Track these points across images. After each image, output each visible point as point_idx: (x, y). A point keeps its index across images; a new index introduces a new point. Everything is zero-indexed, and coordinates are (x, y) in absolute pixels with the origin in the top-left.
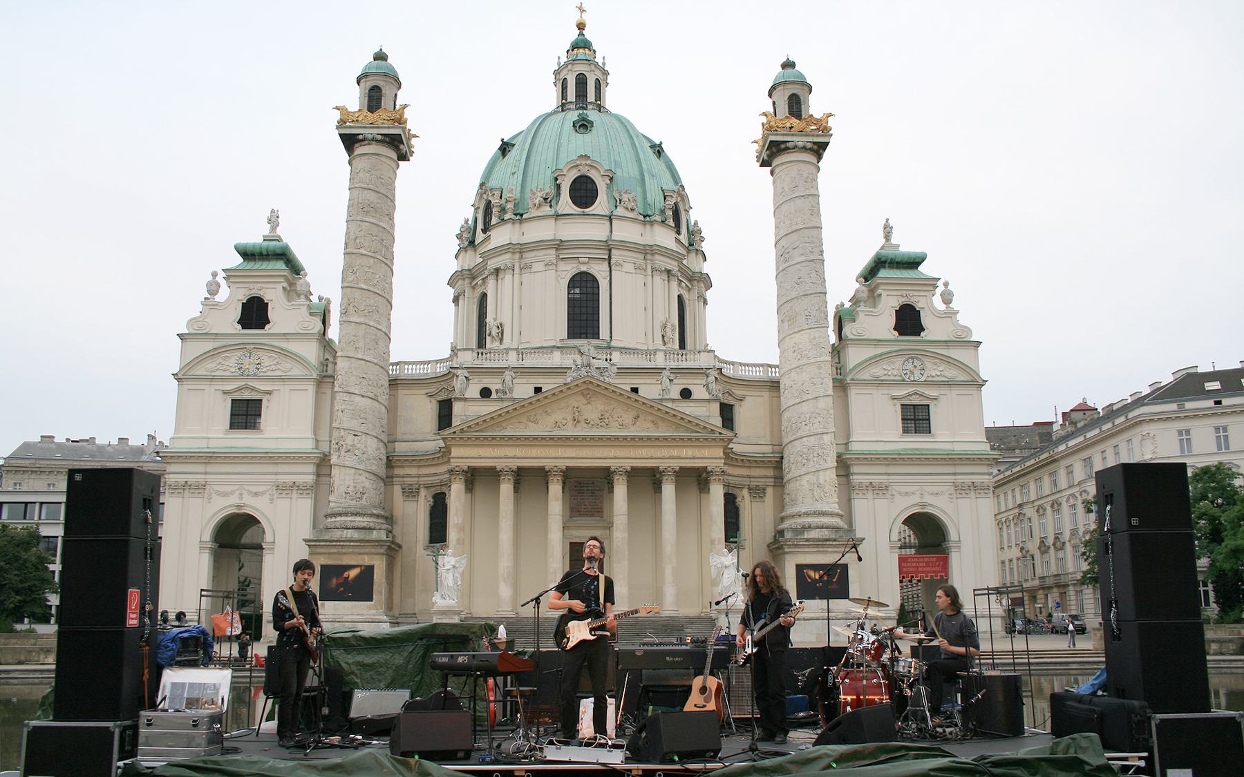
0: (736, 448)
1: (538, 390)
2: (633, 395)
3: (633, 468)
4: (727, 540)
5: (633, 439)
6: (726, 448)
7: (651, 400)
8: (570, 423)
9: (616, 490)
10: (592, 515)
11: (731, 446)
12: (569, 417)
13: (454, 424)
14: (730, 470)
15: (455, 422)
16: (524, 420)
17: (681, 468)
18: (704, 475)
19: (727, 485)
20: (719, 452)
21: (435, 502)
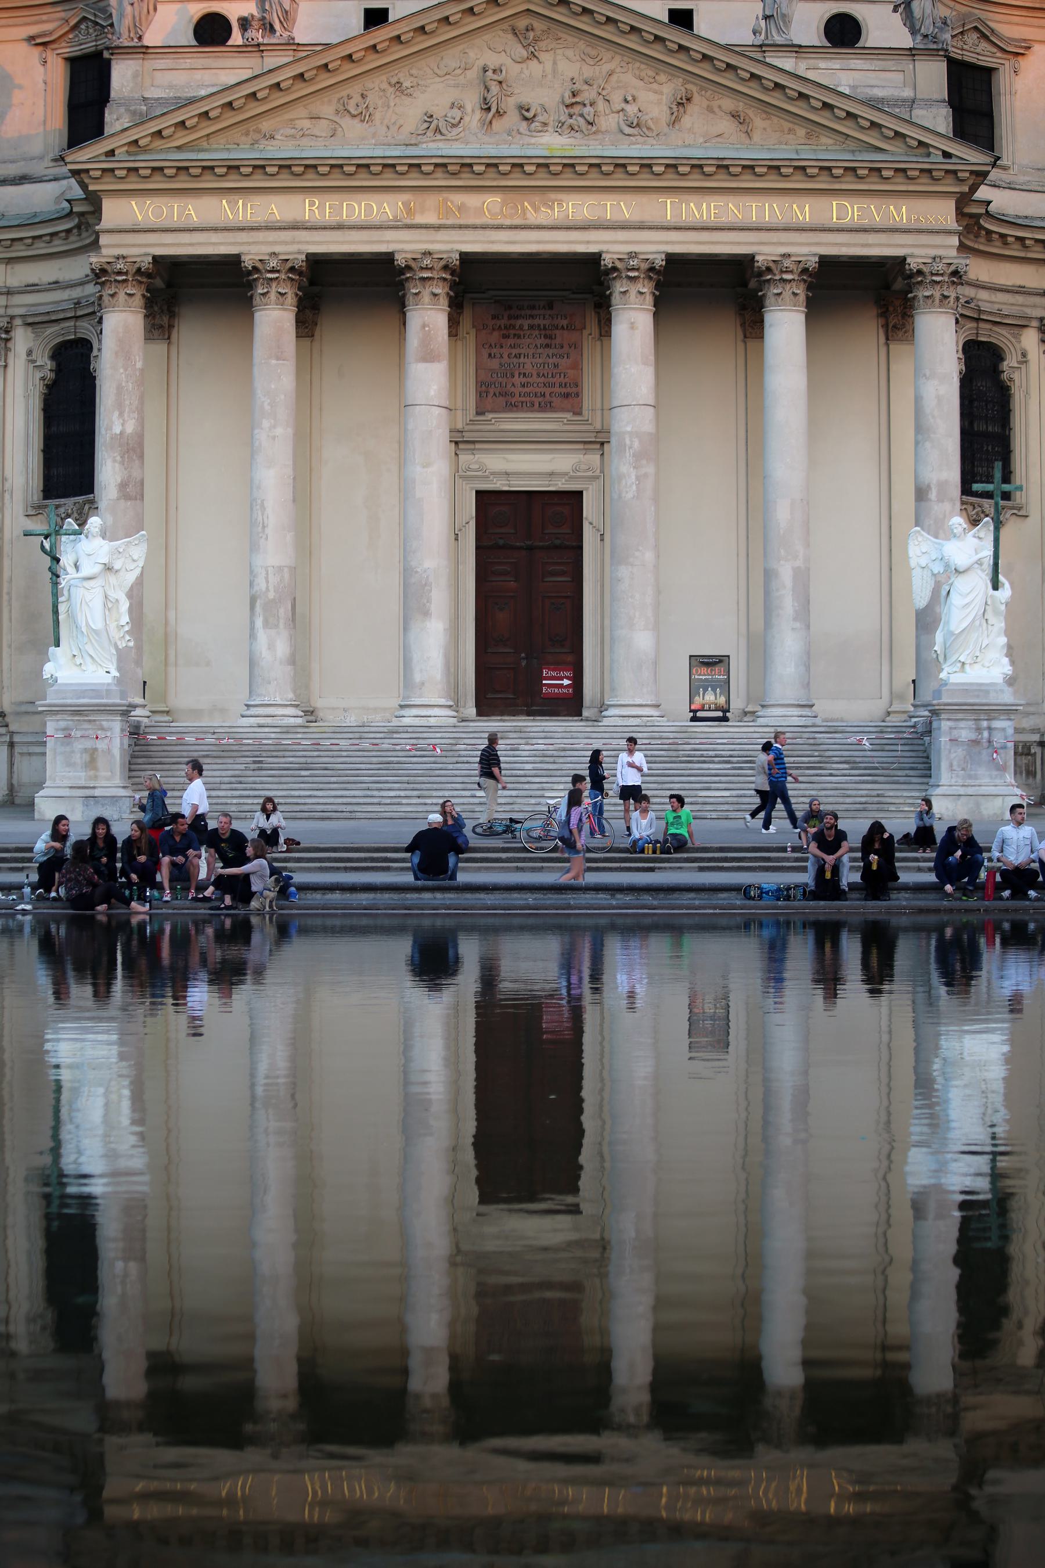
0: (1000, 200)
1: (375, 18)
2: (676, 36)
3: (672, 259)
4: (966, 490)
5: (672, 167)
6: (963, 201)
7: (727, 48)
8: (474, 118)
9: (620, 328)
10: (546, 406)
11: (983, 193)
12: (471, 100)
13: (108, 130)
14: (979, 270)
15: (115, 119)
16: (327, 108)
17: (825, 261)
18: (899, 284)
19: (968, 316)
20: (942, 213)
21: (58, 370)
